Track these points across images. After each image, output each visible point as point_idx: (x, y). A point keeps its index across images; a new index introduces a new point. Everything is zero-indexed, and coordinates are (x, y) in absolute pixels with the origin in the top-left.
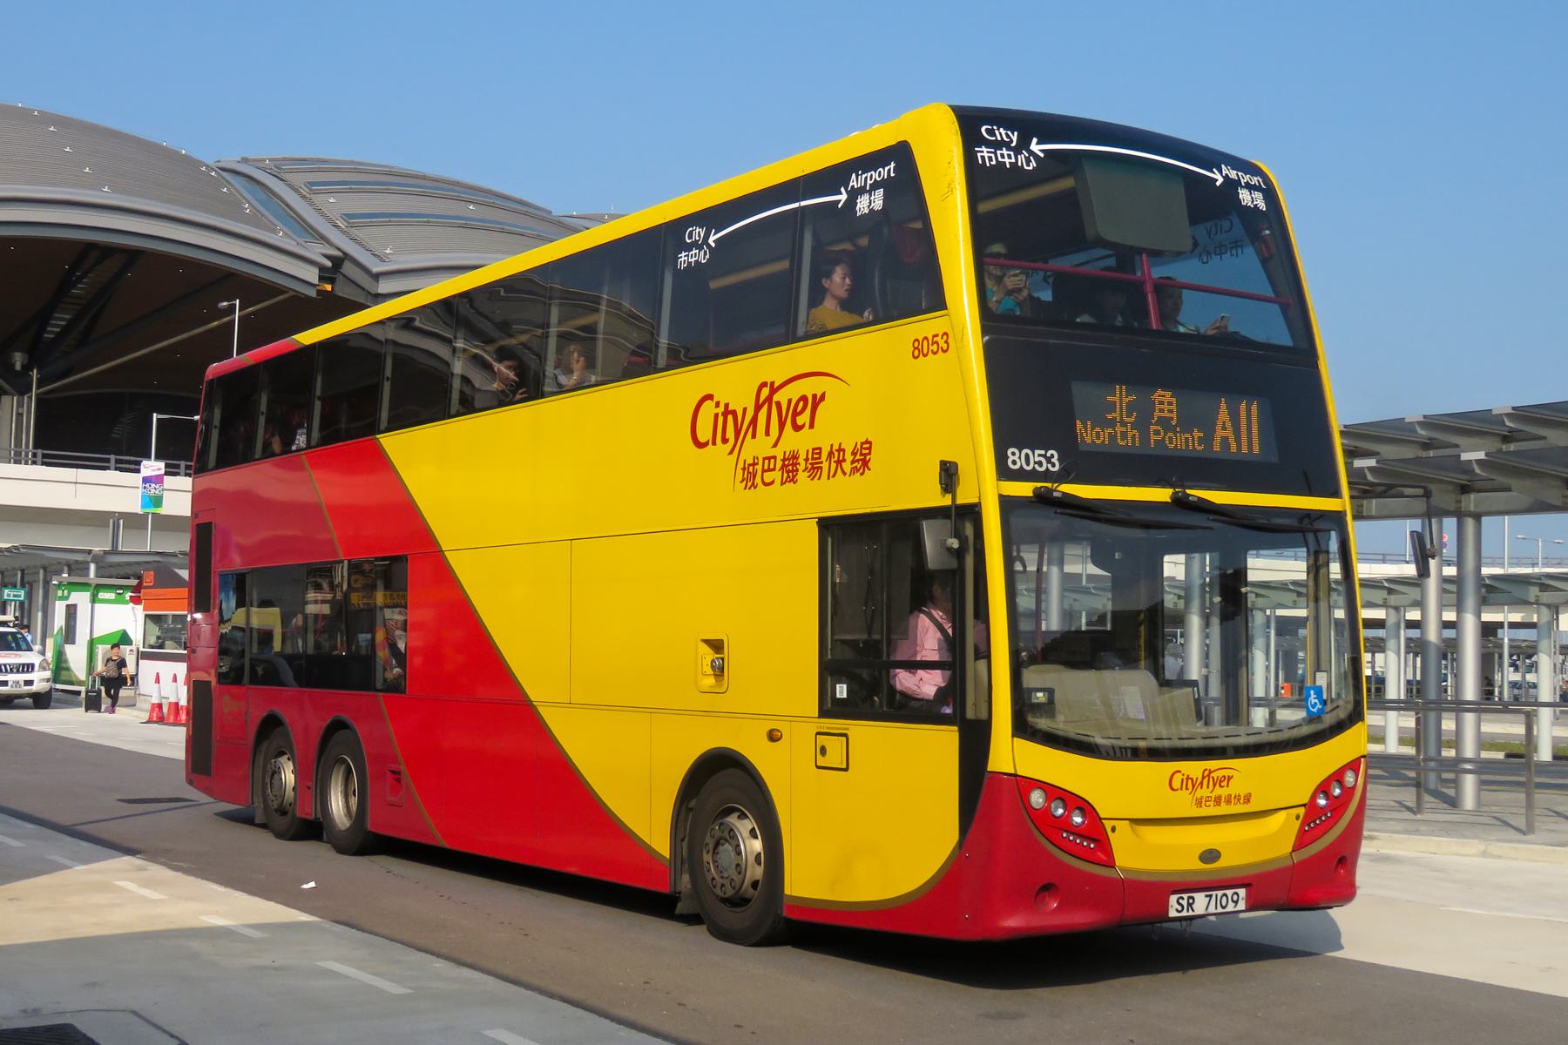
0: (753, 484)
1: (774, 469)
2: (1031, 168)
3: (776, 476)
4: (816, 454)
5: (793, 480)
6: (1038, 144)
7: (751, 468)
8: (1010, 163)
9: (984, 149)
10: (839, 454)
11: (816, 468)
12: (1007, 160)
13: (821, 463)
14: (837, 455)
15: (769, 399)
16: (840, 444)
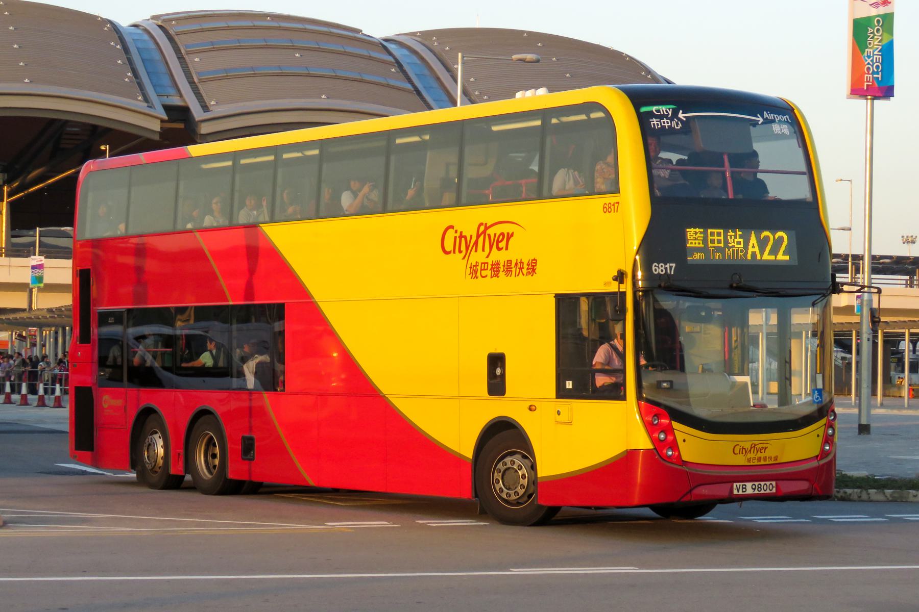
0: (476, 276)
1: (487, 269)
3: (488, 273)
5: (497, 276)
7: (475, 267)
10: (520, 266)
13: (512, 268)
14: (520, 265)
15: (484, 232)
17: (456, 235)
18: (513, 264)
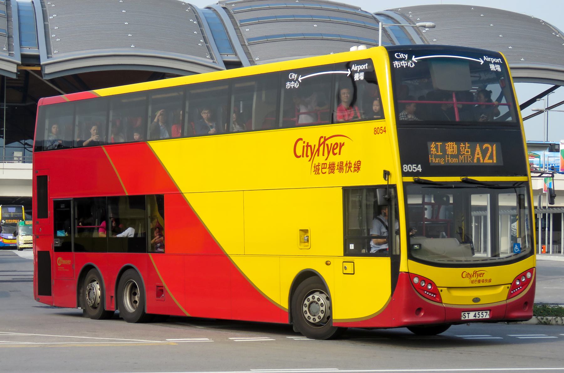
2: (413, 67)
3: (327, 170)
4: (342, 164)
5: (333, 172)
6: (415, 58)
8: (405, 66)
9: (396, 62)
11: (341, 169)
12: (404, 65)
13: (343, 167)
14: (349, 165)
16: (350, 161)
17: (304, 145)
18: (344, 165)
